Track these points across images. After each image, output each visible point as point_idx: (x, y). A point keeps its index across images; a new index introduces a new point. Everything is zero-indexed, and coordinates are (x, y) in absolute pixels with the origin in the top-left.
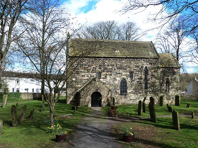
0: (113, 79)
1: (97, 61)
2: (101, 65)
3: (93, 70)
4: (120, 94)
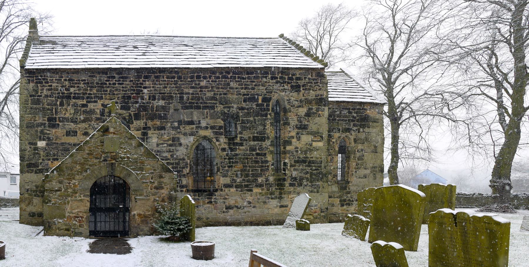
0: (170, 142)
1: (114, 84)
2: (129, 98)
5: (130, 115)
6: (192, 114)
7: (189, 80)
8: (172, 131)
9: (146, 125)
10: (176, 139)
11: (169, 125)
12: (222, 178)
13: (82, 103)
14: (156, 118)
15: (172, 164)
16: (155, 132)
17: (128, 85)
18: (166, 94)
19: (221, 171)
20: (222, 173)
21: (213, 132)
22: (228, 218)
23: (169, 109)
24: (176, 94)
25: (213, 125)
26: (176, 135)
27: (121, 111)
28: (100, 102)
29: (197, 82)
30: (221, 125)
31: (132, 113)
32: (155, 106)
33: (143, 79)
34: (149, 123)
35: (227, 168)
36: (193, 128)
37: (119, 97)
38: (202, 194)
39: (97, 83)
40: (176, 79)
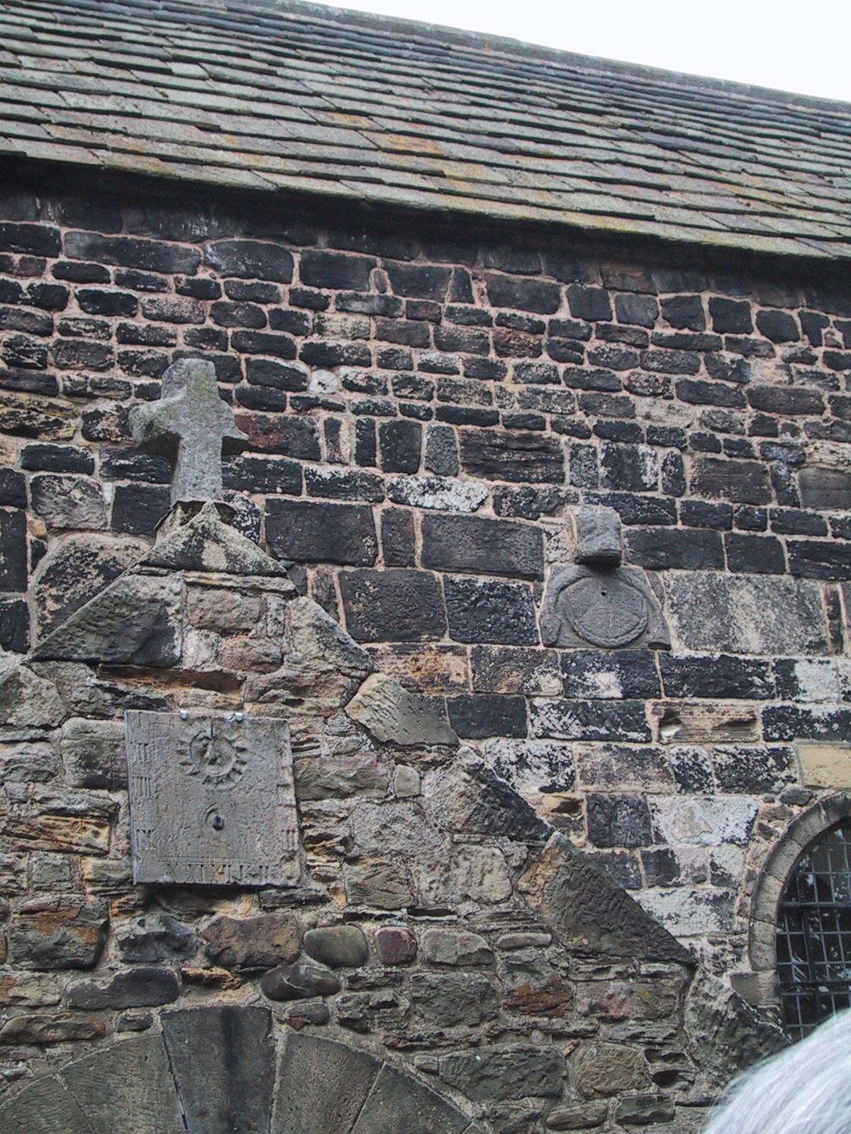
1: (52, 299)
6: (717, 599)
8: (577, 748)
10: (623, 814)
11: (550, 684)
14: (436, 629)
17: (176, 320)
18: (499, 429)
24: (578, 431)
26: (624, 779)
27: (126, 540)
29: (728, 356)
33: (296, 282)
36: (739, 725)
37: (98, 415)
40: (563, 314)
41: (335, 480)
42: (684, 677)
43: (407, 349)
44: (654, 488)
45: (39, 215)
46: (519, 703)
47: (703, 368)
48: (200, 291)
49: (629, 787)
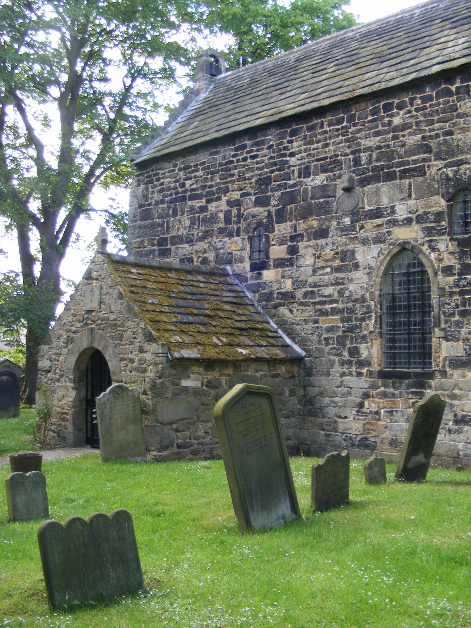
0: (337, 263)
1: (245, 159)
3: (228, 220)
4: (383, 375)
5: (269, 213)
6: (377, 193)
7: (370, 118)
8: (339, 238)
9: (295, 231)
11: (334, 223)
12: (444, 344)
13: (200, 204)
14: (311, 215)
15: (340, 311)
16: (309, 243)
17: (265, 156)
18: (328, 160)
19: (443, 326)
20: (444, 329)
21: (423, 229)
22: (461, 446)
23: (335, 191)
24: (346, 155)
25: (421, 211)
26: (349, 244)
27: (257, 208)
28: (224, 199)
30: (440, 209)
31: (273, 210)
32: (310, 188)
34: (301, 226)
35: (457, 318)
36: (379, 226)
38: (401, 383)
39: (220, 165)
40: (345, 124)
41: (294, 184)
42: (366, 215)
43: (309, 146)
44: (364, 165)
45: (244, 141)
46: (328, 230)
47: (380, 126)
48: (270, 147)
49: (351, 247)
